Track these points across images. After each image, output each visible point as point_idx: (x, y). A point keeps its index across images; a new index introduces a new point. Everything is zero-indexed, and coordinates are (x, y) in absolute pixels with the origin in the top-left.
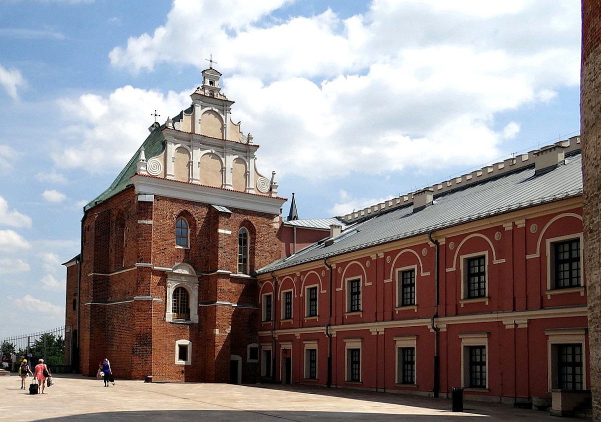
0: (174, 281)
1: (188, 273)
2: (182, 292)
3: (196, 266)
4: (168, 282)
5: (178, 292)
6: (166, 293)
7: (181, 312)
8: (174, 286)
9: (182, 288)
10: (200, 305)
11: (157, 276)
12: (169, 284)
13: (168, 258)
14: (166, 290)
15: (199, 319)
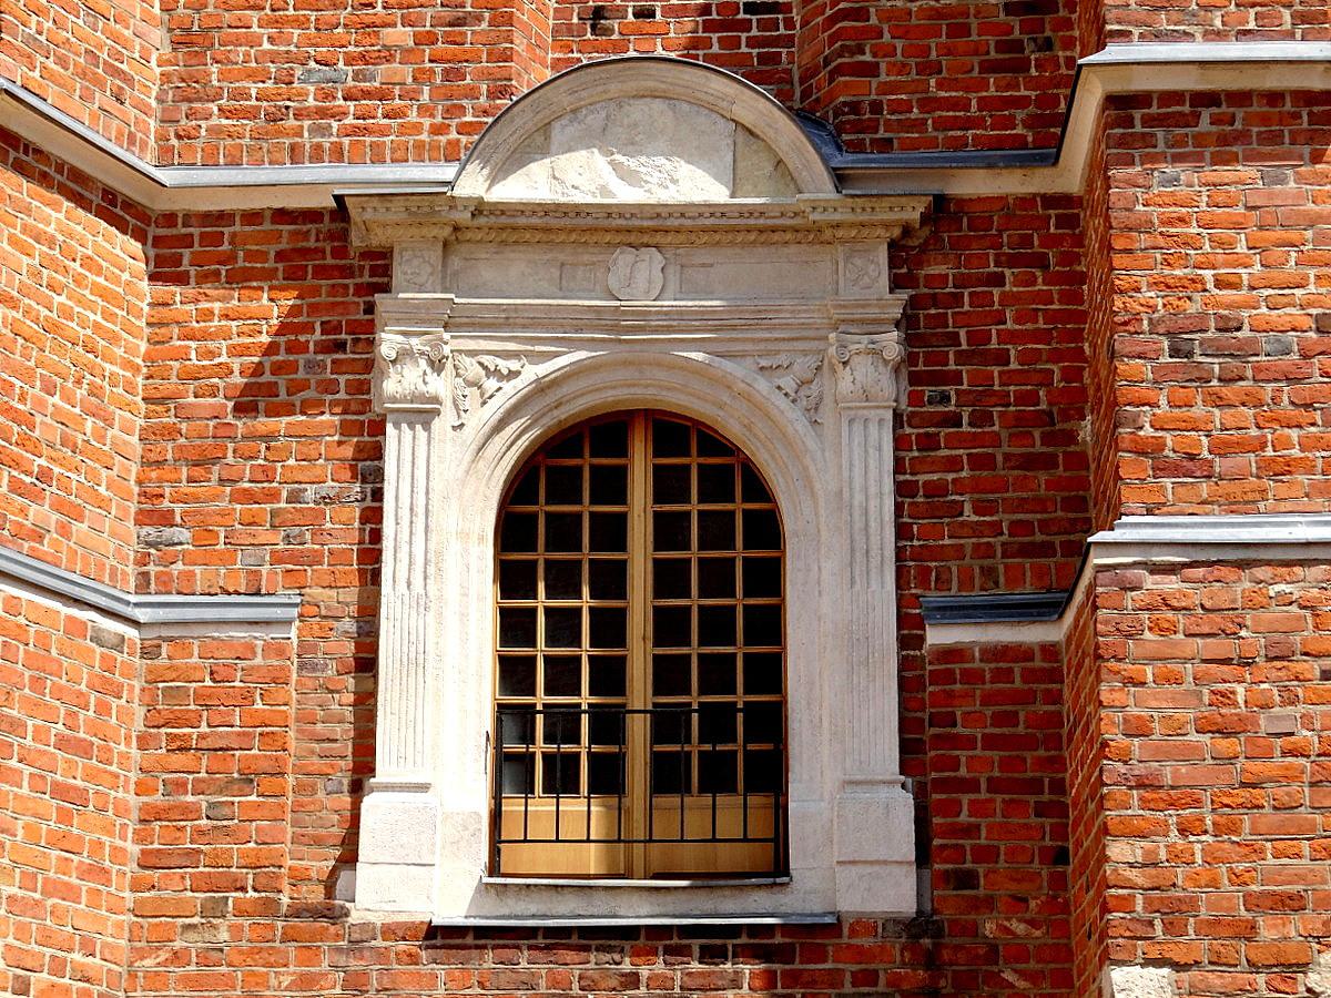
0: (504, 322)
1: (717, 193)
2: (667, 485)
3: (848, 90)
4: (389, 342)
5: (613, 486)
6: (373, 516)
7: (667, 776)
8: (512, 390)
9: (672, 431)
10: (938, 636)
11: (239, 279)
12: (399, 384)
13: (401, 35)
14: (368, 467)
15: (924, 855)
